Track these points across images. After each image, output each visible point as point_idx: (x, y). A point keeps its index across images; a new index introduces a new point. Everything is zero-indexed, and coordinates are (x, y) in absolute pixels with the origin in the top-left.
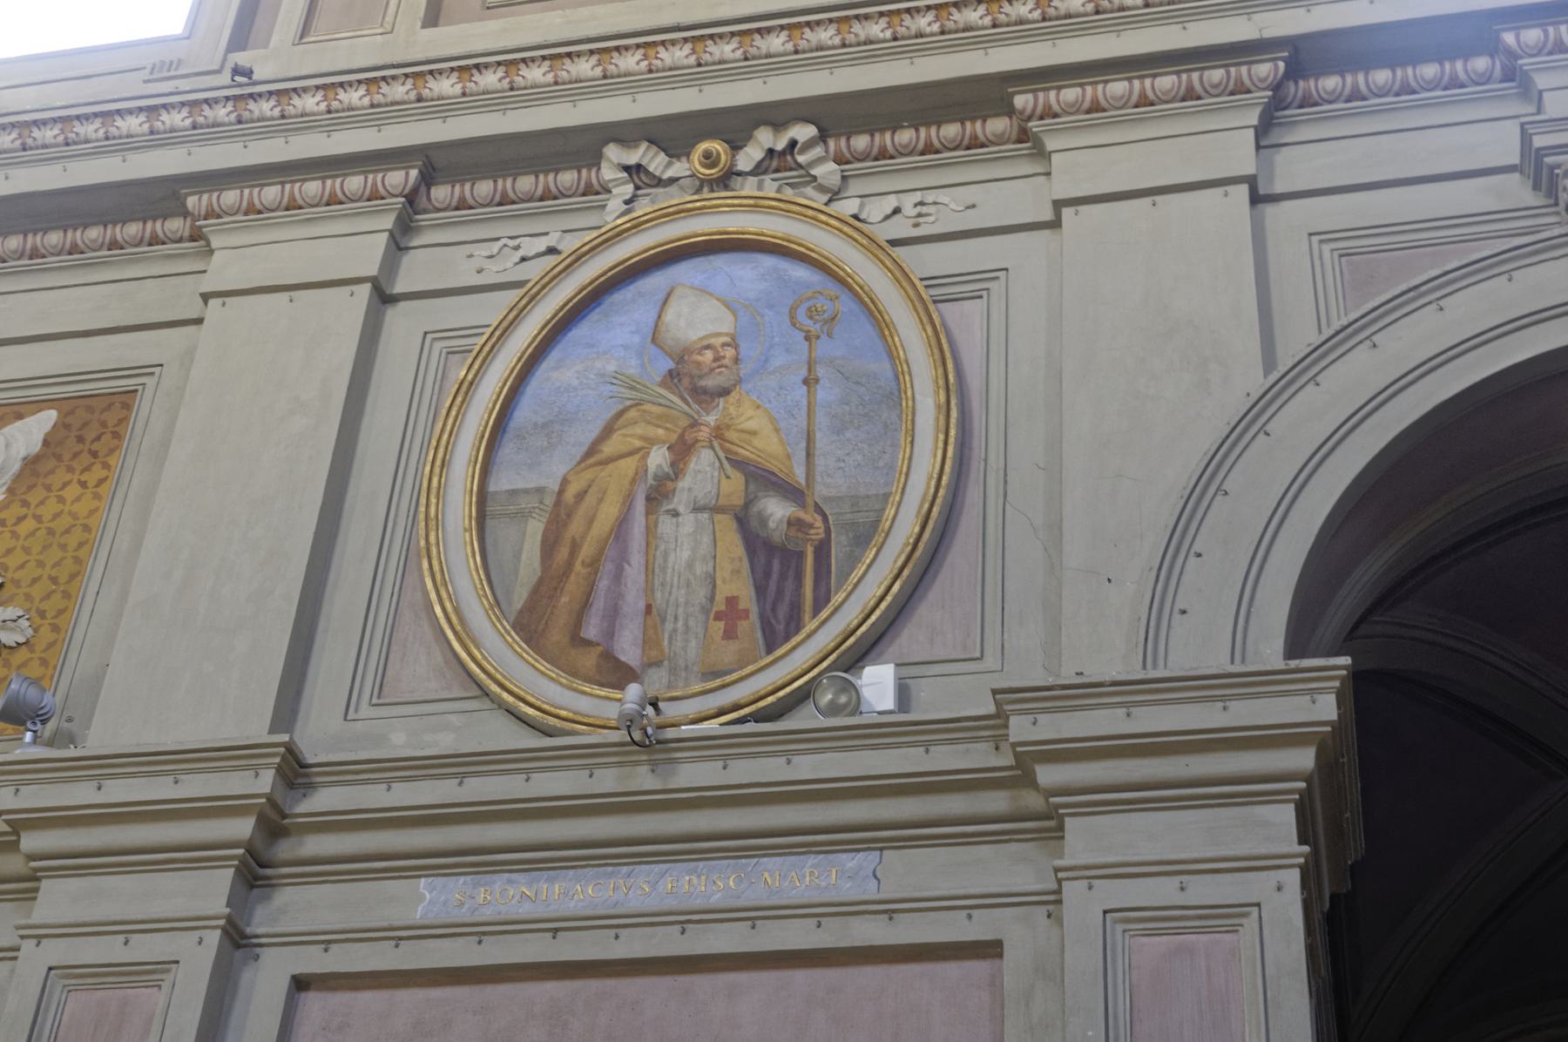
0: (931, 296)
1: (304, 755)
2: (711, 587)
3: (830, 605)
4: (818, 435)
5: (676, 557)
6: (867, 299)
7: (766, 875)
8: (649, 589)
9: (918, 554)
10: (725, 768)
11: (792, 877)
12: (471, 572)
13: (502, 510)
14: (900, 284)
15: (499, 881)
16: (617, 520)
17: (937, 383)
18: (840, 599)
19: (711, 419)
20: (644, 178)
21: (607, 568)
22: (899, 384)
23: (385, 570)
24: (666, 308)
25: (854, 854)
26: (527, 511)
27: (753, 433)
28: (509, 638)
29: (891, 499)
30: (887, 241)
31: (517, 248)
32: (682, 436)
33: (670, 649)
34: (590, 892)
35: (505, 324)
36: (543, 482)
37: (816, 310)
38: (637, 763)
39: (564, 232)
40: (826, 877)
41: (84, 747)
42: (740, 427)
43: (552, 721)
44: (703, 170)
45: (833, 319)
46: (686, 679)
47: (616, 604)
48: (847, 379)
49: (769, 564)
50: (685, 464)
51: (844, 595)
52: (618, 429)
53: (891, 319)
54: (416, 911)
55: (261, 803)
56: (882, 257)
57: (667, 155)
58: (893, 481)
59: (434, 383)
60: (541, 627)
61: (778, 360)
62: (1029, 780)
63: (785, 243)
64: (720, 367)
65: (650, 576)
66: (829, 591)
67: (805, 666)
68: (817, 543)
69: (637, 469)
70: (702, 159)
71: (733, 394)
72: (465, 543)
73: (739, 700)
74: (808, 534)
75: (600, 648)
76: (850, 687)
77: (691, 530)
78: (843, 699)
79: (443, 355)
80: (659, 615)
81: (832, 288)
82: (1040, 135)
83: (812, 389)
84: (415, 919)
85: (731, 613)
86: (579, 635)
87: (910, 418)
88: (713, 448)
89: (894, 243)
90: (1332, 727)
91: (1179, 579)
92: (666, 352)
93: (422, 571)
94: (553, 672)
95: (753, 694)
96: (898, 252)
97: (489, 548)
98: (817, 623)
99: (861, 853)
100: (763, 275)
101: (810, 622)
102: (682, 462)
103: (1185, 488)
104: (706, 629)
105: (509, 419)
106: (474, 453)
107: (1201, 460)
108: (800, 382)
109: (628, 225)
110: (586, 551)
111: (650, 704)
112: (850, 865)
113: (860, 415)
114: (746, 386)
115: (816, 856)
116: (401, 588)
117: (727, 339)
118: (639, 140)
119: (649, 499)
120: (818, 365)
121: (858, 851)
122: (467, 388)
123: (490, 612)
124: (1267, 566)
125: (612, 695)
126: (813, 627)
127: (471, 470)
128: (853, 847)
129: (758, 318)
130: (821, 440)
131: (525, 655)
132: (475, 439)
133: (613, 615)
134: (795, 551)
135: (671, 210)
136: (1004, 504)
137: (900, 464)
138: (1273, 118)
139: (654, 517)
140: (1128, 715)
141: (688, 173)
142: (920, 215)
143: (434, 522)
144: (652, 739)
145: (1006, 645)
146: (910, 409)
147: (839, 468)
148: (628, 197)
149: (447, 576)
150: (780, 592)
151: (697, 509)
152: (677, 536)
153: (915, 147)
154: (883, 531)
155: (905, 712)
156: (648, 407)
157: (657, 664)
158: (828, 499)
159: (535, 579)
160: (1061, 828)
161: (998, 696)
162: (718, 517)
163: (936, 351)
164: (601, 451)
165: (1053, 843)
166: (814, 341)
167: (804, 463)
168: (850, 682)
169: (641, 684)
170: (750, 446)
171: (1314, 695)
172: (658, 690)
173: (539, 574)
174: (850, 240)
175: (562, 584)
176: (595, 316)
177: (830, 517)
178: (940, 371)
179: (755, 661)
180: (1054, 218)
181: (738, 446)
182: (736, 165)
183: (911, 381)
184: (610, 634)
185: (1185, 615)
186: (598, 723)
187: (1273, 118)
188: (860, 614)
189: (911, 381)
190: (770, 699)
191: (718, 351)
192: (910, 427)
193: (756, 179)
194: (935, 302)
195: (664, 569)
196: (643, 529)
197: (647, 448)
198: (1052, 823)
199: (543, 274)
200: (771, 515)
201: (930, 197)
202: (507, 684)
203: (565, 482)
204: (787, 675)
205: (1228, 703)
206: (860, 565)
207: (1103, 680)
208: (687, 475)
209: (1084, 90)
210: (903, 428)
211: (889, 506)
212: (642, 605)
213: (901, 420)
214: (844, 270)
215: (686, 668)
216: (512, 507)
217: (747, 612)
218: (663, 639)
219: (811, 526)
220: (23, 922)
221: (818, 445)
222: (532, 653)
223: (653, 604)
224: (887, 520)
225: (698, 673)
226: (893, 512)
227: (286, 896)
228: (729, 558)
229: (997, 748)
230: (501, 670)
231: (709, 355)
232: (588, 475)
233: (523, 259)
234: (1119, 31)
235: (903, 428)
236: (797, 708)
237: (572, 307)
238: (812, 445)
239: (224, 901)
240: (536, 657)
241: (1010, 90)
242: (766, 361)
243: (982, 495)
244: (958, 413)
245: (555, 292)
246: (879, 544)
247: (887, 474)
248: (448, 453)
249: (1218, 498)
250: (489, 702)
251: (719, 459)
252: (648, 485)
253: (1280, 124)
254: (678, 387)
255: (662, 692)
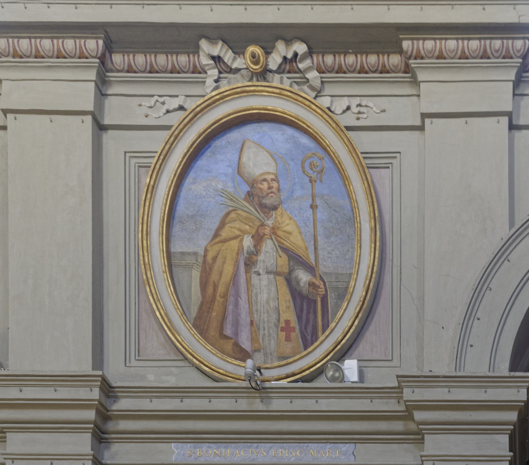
0: (366, 164)
1: (110, 382)
2: (278, 314)
3: (329, 328)
4: (319, 238)
5: (261, 297)
6: (337, 162)
7: (311, 451)
8: (251, 313)
9: (365, 306)
10: (291, 402)
11: (322, 453)
12: (169, 295)
13: (180, 263)
14: (352, 154)
15: (205, 446)
16: (233, 274)
17: (370, 215)
18: (333, 326)
19: (270, 223)
20: (222, 66)
21: (231, 299)
22: (353, 214)
23: (129, 290)
24: (242, 153)
25: (345, 444)
26: (191, 264)
27: (290, 233)
28: (192, 332)
29: (353, 276)
30: (345, 127)
31: (163, 103)
32: (257, 231)
33: (263, 343)
34: (242, 454)
35: (164, 152)
36: (196, 249)
37: (314, 165)
38: (255, 397)
39: (187, 96)
40: (335, 454)
41: (8, 370)
42: (284, 229)
43: (217, 375)
44: (252, 66)
45: (322, 171)
46: (272, 359)
47: (237, 319)
48: (330, 207)
49: (302, 305)
50: (260, 247)
51: (335, 324)
52: (228, 223)
53: (349, 176)
54: (173, 458)
55: (96, 404)
56: (343, 137)
57: (233, 52)
58: (353, 267)
59: (135, 184)
60: (205, 328)
61: (298, 193)
62: (410, 418)
63: (296, 121)
64: (271, 193)
65: (251, 306)
66: (328, 321)
67: (321, 357)
68: (322, 296)
69: (238, 247)
70: (251, 58)
71: (279, 209)
72: (165, 279)
73: (294, 371)
74: (318, 291)
75: (233, 341)
76: (339, 369)
77: (266, 283)
78: (337, 375)
79: (137, 167)
80: (257, 326)
81: (321, 153)
82: (415, 69)
83: (315, 211)
84: (172, 461)
85: (287, 328)
86: (223, 333)
87: (359, 233)
88: (272, 239)
89: (349, 128)
90: (524, 403)
91: (470, 330)
92: (245, 180)
93: (147, 293)
94: (214, 351)
95: (300, 369)
96: (350, 134)
97: (176, 283)
98: (324, 337)
99: (348, 444)
100: (287, 139)
101: (321, 336)
102: (259, 246)
103: (474, 285)
104: (278, 335)
105: (175, 211)
106: (161, 229)
107: (481, 271)
108: (309, 207)
109: (218, 97)
110: (221, 290)
111: (258, 370)
112: (343, 449)
113: (337, 229)
114: (285, 206)
115: (330, 444)
116: (139, 300)
117: (273, 177)
118: (217, 39)
119: (246, 264)
120: (316, 198)
121: (346, 443)
122: (152, 189)
123: (182, 317)
124: (505, 327)
125: (241, 364)
126: (323, 339)
127: (161, 238)
128: (345, 441)
129: (287, 166)
130: (321, 241)
131: (200, 341)
132: (160, 221)
133: (236, 324)
134: (313, 299)
135: (238, 90)
136: (400, 284)
137: (355, 258)
138: (522, 77)
139: (250, 274)
140: (449, 391)
141: (245, 66)
142: (359, 113)
143: (148, 266)
144: (260, 387)
145: (402, 355)
146: (359, 229)
147: (329, 257)
148: (216, 78)
149: (159, 296)
150: (308, 320)
151: (268, 273)
152: (260, 286)
153: (356, 67)
154: (349, 293)
155: (362, 383)
156: (240, 212)
157: (258, 350)
158: (325, 273)
159: (199, 302)
160: (423, 439)
161: (399, 379)
162: (278, 278)
163: (369, 197)
164: (221, 235)
165: (420, 445)
166: (314, 183)
167: (314, 253)
168: (340, 367)
169: (253, 360)
170: (289, 240)
171: (519, 389)
172: (260, 363)
173: (201, 300)
174: (327, 123)
175: (212, 306)
176: (208, 153)
177: (326, 283)
178: (371, 208)
179: (299, 353)
180: (421, 124)
181: (283, 239)
182: (268, 65)
183: (359, 213)
184: (236, 334)
185: (472, 347)
186: (236, 377)
187: (522, 77)
188: (342, 334)
189: (359, 213)
190: (307, 372)
191: (270, 183)
192: (359, 238)
193: (279, 76)
194: (368, 167)
195: (256, 302)
196: (245, 280)
197: (242, 236)
198: (419, 437)
199: (179, 123)
200: (301, 279)
201: (364, 101)
202: (195, 355)
203: (206, 251)
204: (313, 361)
205: (487, 389)
206: (341, 309)
207: (440, 375)
208: (262, 253)
209: (436, 43)
210: (356, 239)
211: (352, 280)
212: (248, 320)
213: (355, 234)
214: (325, 142)
215: (271, 354)
216: (183, 262)
217: (294, 328)
218: (260, 338)
219: (319, 287)
220: (3, 452)
221: (319, 244)
222: (203, 340)
223: (254, 320)
224: (351, 287)
225: (276, 357)
226: (353, 283)
227: (116, 447)
228: (284, 300)
229: (399, 402)
230: (191, 347)
231: (265, 186)
232: (216, 248)
233: (168, 112)
234: (453, 5)
235: (356, 239)
236: (319, 377)
237: (196, 146)
238: (316, 243)
239: (90, 448)
240: (206, 342)
241: (401, 36)
242: (292, 192)
243: (391, 279)
244: (380, 234)
245: (186, 135)
246: (348, 300)
247: (350, 263)
248: (149, 228)
249: (488, 291)
250: (188, 363)
251: (275, 246)
252: (245, 257)
253: (525, 81)
254: (252, 202)
255: (262, 364)
